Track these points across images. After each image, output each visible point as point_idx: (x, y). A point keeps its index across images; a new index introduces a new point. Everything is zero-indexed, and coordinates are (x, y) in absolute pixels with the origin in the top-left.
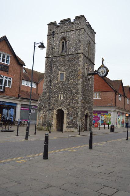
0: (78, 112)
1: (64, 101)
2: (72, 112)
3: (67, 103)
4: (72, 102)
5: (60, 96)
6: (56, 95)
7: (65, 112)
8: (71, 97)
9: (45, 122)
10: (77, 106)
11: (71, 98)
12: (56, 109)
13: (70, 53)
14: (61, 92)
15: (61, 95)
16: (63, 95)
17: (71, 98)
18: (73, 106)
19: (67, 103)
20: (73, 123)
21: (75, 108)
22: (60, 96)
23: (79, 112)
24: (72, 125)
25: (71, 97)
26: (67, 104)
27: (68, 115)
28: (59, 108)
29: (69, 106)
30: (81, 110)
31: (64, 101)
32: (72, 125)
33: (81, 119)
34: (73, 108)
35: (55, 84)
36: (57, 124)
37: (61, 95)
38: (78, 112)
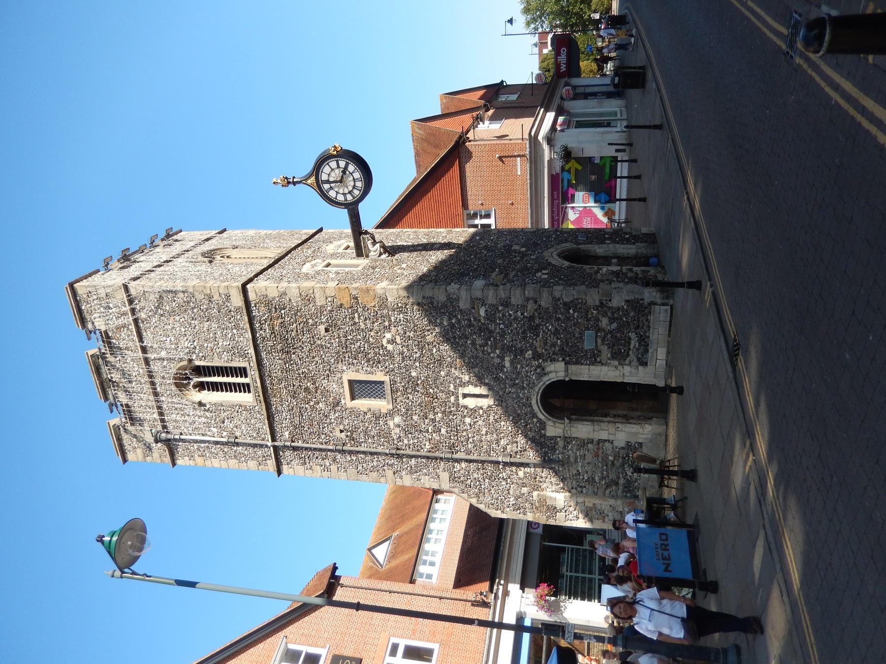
0: (556, 300)
1: (497, 379)
2: (556, 333)
3: (507, 364)
4: (503, 334)
5: (471, 403)
6: (468, 420)
7: (557, 371)
8: (474, 343)
9: (617, 484)
10: (524, 307)
11: (479, 342)
12: (543, 426)
13: (252, 351)
14: (449, 393)
15: (465, 396)
16: (463, 385)
17: (479, 342)
18: (524, 332)
19: (507, 364)
20: (618, 329)
21: (531, 318)
22: (471, 403)
23: (557, 294)
24: (632, 335)
25: (474, 343)
26: (512, 362)
27: (572, 354)
28: (535, 407)
29: (522, 352)
30: (545, 284)
31: (497, 379)
32: (632, 335)
33: (594, 283)
34: (535, 329)
35: (409, 429)
36: (627, 419)
37: (465, 396)
38: (556, 300)
